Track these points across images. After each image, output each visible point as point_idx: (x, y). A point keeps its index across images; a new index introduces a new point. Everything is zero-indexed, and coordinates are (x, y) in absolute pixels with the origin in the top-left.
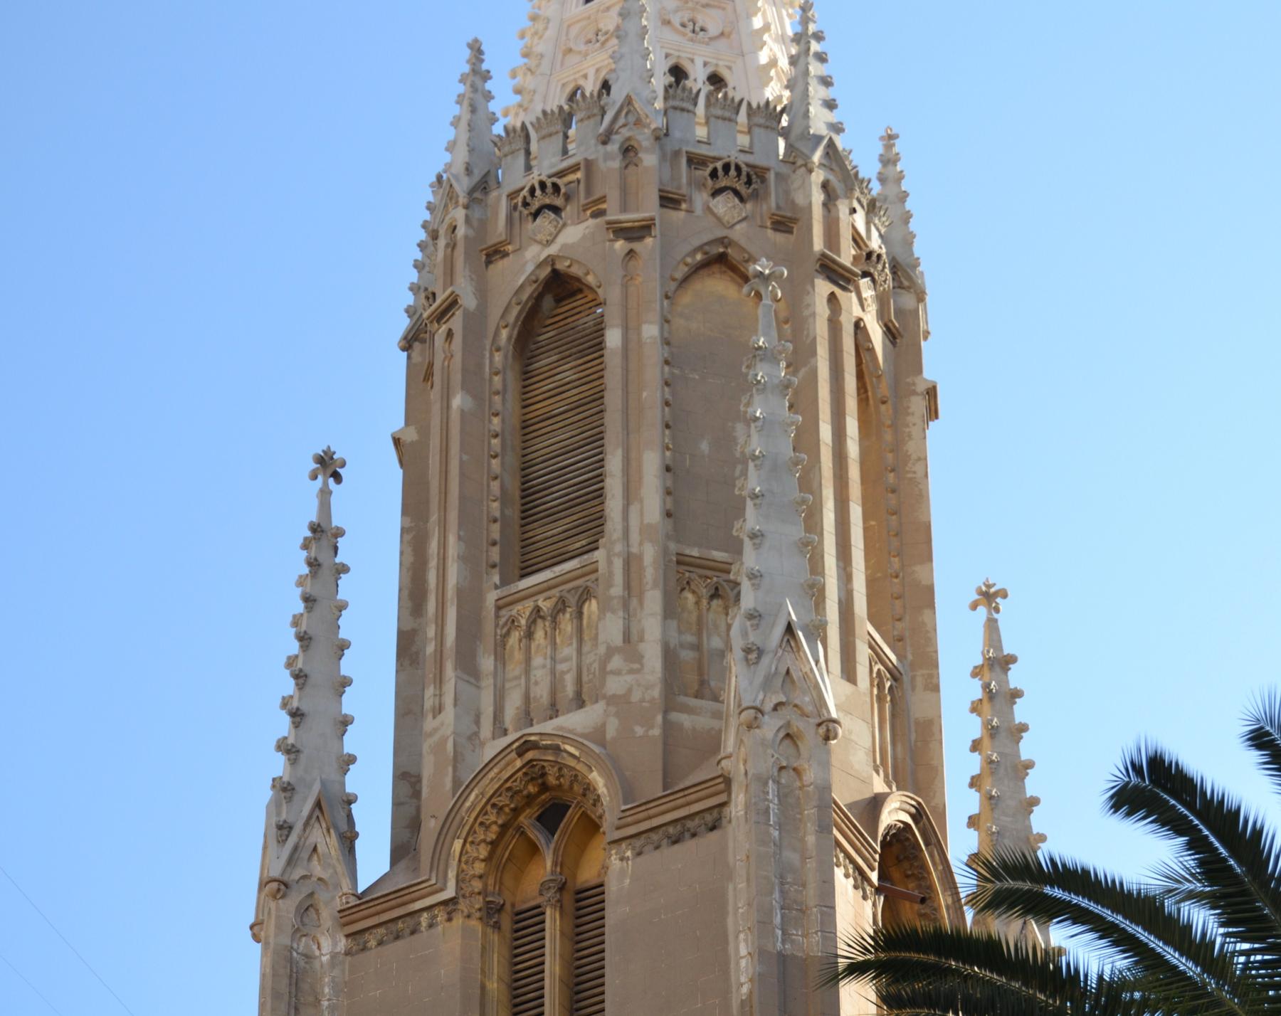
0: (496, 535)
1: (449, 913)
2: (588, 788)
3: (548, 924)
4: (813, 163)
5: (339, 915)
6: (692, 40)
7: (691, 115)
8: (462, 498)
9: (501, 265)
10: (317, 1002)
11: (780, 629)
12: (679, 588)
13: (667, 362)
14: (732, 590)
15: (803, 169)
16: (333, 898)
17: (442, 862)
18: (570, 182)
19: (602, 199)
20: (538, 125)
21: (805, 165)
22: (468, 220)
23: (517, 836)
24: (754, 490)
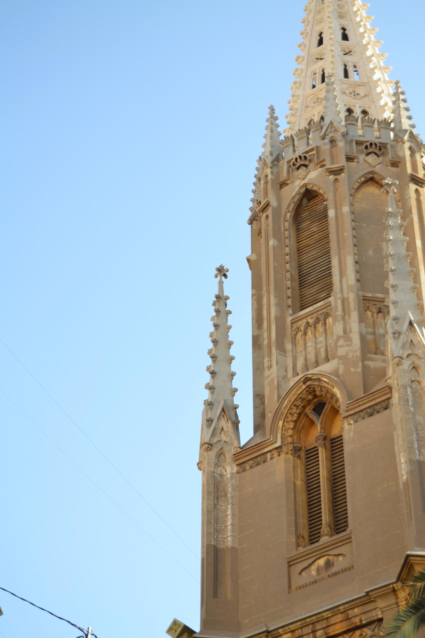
0: (289, 294)
1: (279, 453)
2: (333, 395)
3: (320, 455)
4: (405, 140)
5: (233, 456)
6: (354, 99)
7: (356, 126)
8: (275, 280)
9: (286, 189)
10: (226, 495)
11: (407, 324)
12: (364, 310)
13: (353, 221)
14: (386, 309)
15: (401, 143)
16: (231, 449)
17: (275, 431)
18: (311, 155)
19: (324, 160)
20: (297, 135)
21: (402, 141)
22: (272, 173)
23: (305, 418)
24: (392, 268)
